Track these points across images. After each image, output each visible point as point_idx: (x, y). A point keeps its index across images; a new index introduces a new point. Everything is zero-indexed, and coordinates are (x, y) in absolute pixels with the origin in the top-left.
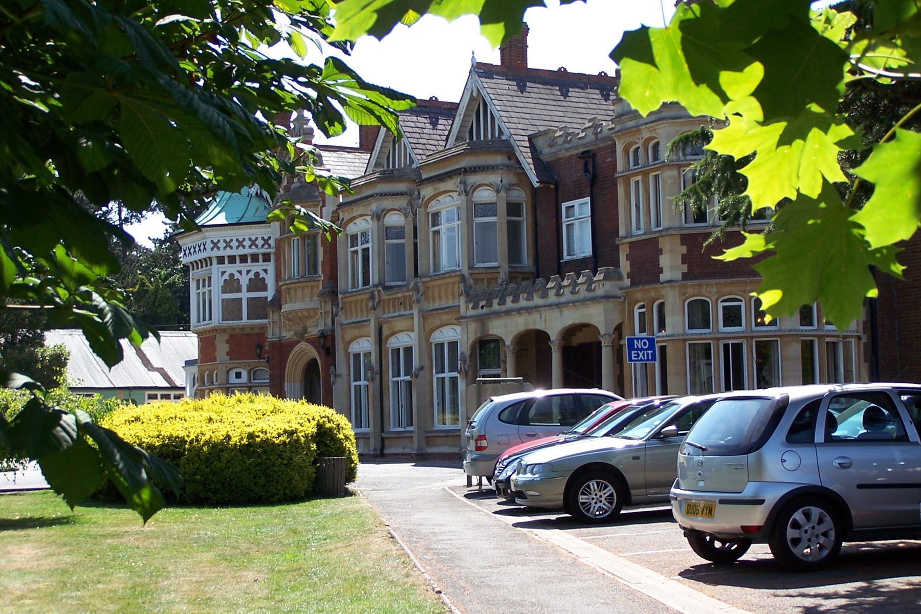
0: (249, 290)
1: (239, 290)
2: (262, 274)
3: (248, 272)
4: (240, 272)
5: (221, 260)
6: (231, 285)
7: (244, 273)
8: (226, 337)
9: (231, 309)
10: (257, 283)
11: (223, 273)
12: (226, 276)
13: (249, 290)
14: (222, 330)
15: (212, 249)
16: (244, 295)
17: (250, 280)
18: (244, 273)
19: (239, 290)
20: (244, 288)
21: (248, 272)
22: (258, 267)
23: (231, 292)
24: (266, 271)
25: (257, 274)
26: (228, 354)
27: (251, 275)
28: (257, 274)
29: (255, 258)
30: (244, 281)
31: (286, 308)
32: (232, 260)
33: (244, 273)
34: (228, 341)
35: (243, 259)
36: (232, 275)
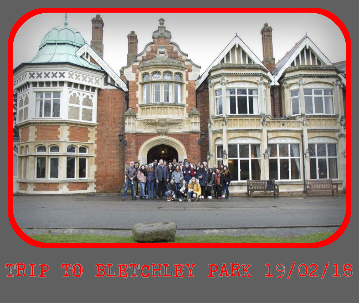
0: (84, 104)
1: (78, 103)
2: (90, 98)
3: (84, 94)
4: (79, 94)
5: (70, 84)
6: (74, 99)
7: (81, 94)
8: (68, 127)
9: (74, 112)
10: (88, 102)
11: (70, 92)
12: (72, 94)
13: (84, 104)
14: (66, 123)
15: (69, 77)
16: (81, 107)
17: (84, 98)
18: (82, 95)
19: (78, 103)
20: (81, 103)
21: (84, 94)
22: (89, 93)
23: (74, 103)
24: (92, 96)
25: (88, 97)
26: (69, 137)
27: (85, 97)
28: (88, 97)
29: (88, 88)
30: (81, 99)
31: (141, 115)
32: (76, 85)
33: (81, 94)
34: (69, 130)
35: (82, 86)
36: (75, 94)
